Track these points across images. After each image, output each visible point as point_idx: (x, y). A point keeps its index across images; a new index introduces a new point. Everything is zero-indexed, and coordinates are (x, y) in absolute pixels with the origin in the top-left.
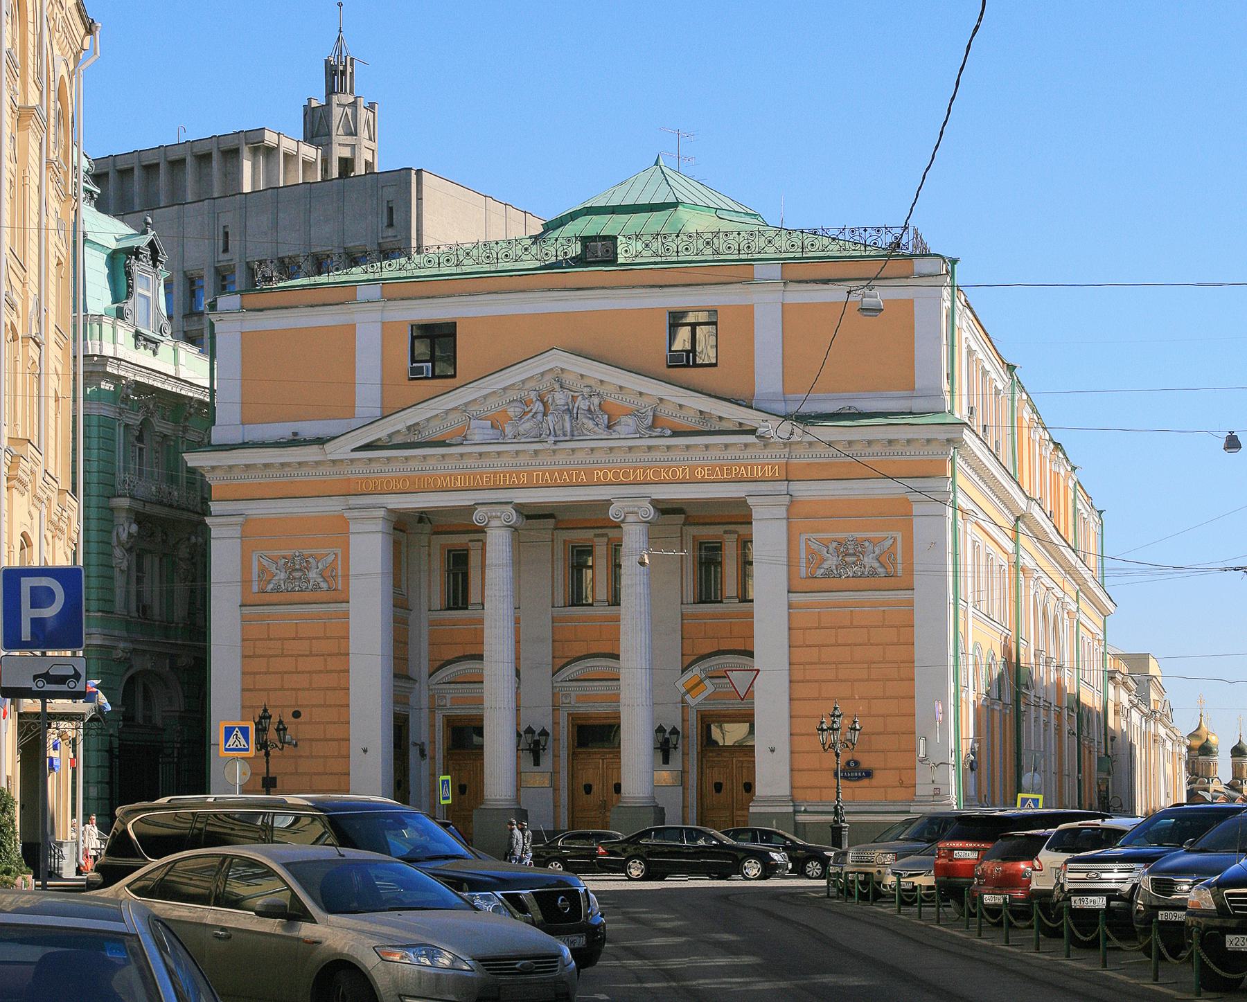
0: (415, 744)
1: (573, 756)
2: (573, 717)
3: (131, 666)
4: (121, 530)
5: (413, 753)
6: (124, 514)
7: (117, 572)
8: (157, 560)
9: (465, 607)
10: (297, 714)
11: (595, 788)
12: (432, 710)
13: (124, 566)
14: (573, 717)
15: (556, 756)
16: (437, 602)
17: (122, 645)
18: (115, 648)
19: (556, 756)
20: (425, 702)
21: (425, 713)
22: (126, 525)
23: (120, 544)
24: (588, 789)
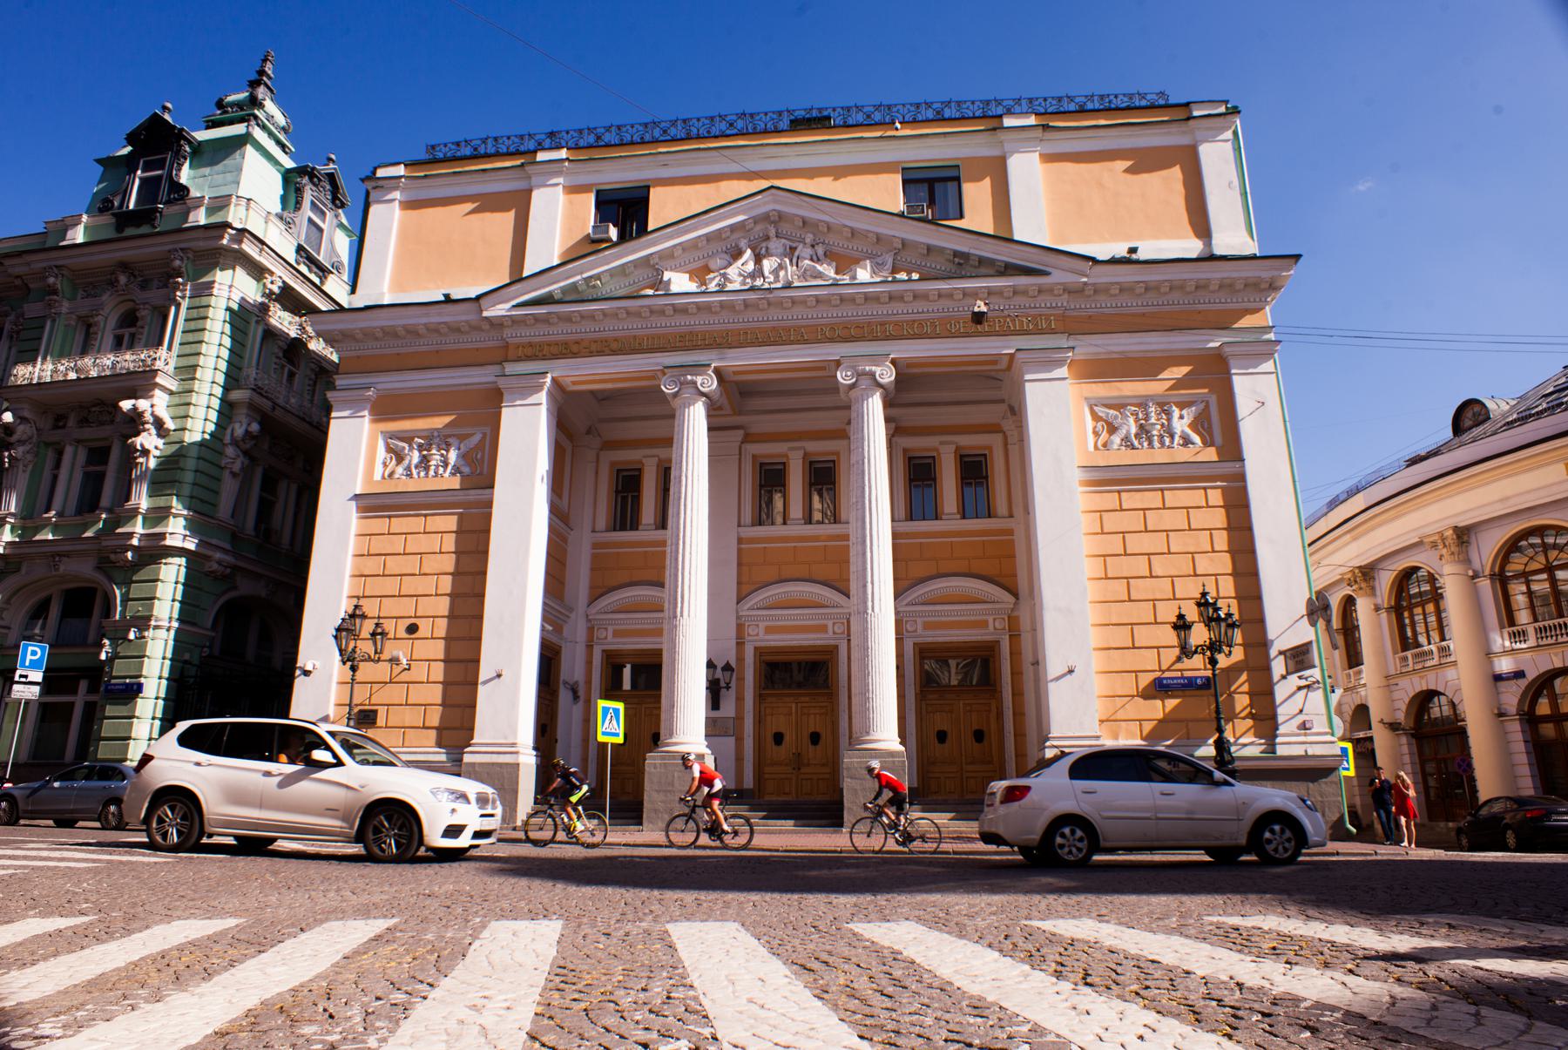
0: (565, 683)
1: (760, 698)
2: (760, 652)
3: (235, 588)
4: (237, 426)
5: (564, 696)
6: (245, 411)
7: (226, 475)
8: (294, 488)
9: (635, 526)
10: (412, 629)
11: (787, 738)
12: (590, 647)
13: (237, 467)
14: (760, 652)
15: (740, 699)
16: (602, 522)
17: (218, 555)
18: (208, 558)
19: (740, 699)
20: (581, 635)
21: (580, 650)
22: (245, 421)
23: (235, 442)
24: (778, 738)
